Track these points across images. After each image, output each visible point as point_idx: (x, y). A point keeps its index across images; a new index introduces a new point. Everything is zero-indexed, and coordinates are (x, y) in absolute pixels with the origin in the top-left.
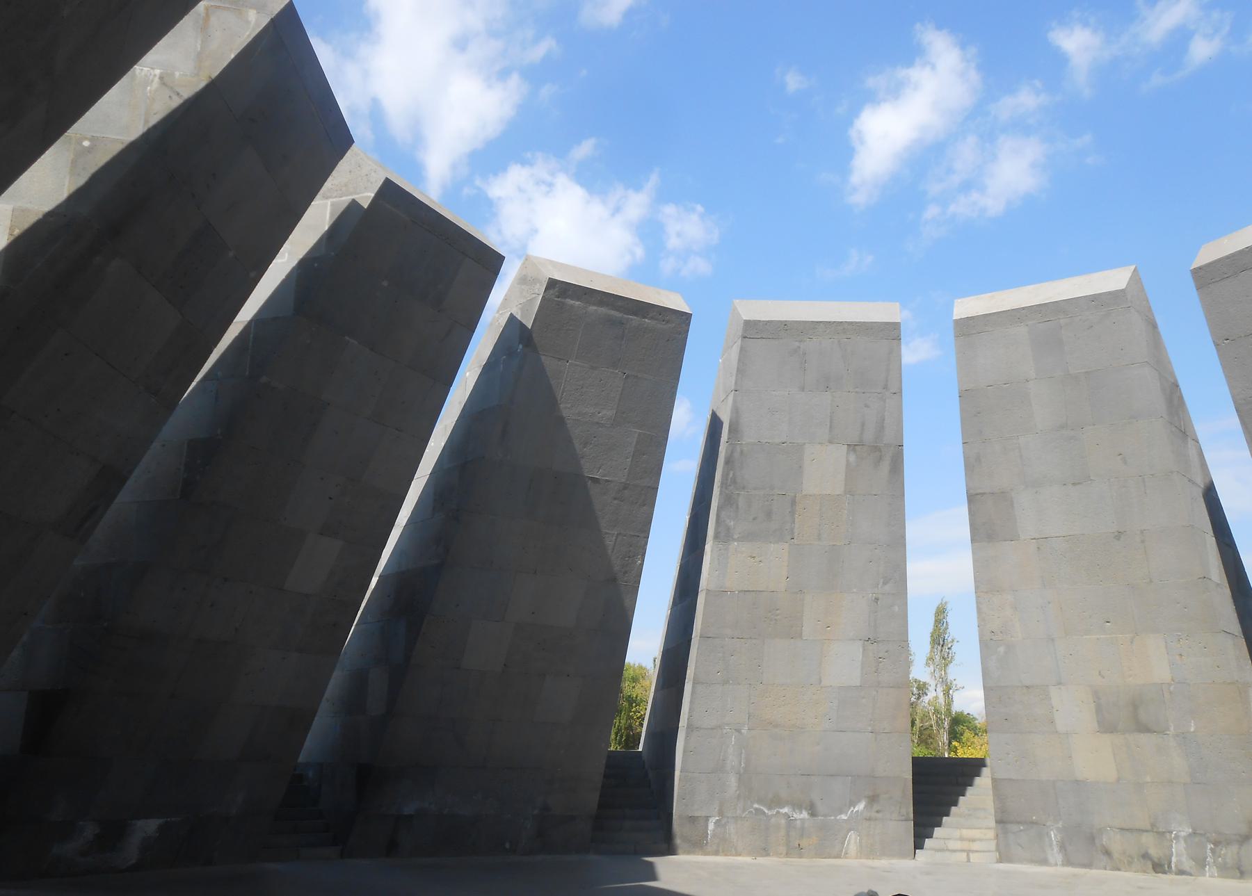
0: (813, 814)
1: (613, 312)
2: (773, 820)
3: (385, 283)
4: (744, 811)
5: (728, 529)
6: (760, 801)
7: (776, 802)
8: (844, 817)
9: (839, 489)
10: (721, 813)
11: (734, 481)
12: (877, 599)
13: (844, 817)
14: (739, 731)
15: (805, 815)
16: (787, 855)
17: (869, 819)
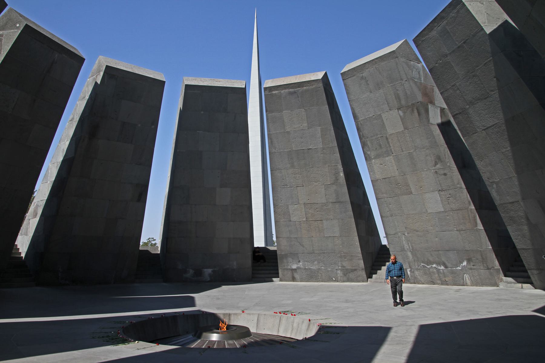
0: (446, 267)
1: (291, 90)
2: (431, 270)
3: (202, 112)
4: (418, 266)
5: (369, 155)
6: (423, 262)
7: (429, 263)
8: (459, 268)
9: (402, 129)
10: (410, 267)
11: (363, 136)
12: (436, 172)
13: (459, 268)
14: (404, 234)
15: (442, 268)
16: (442, 284)
17: (471, 269)
